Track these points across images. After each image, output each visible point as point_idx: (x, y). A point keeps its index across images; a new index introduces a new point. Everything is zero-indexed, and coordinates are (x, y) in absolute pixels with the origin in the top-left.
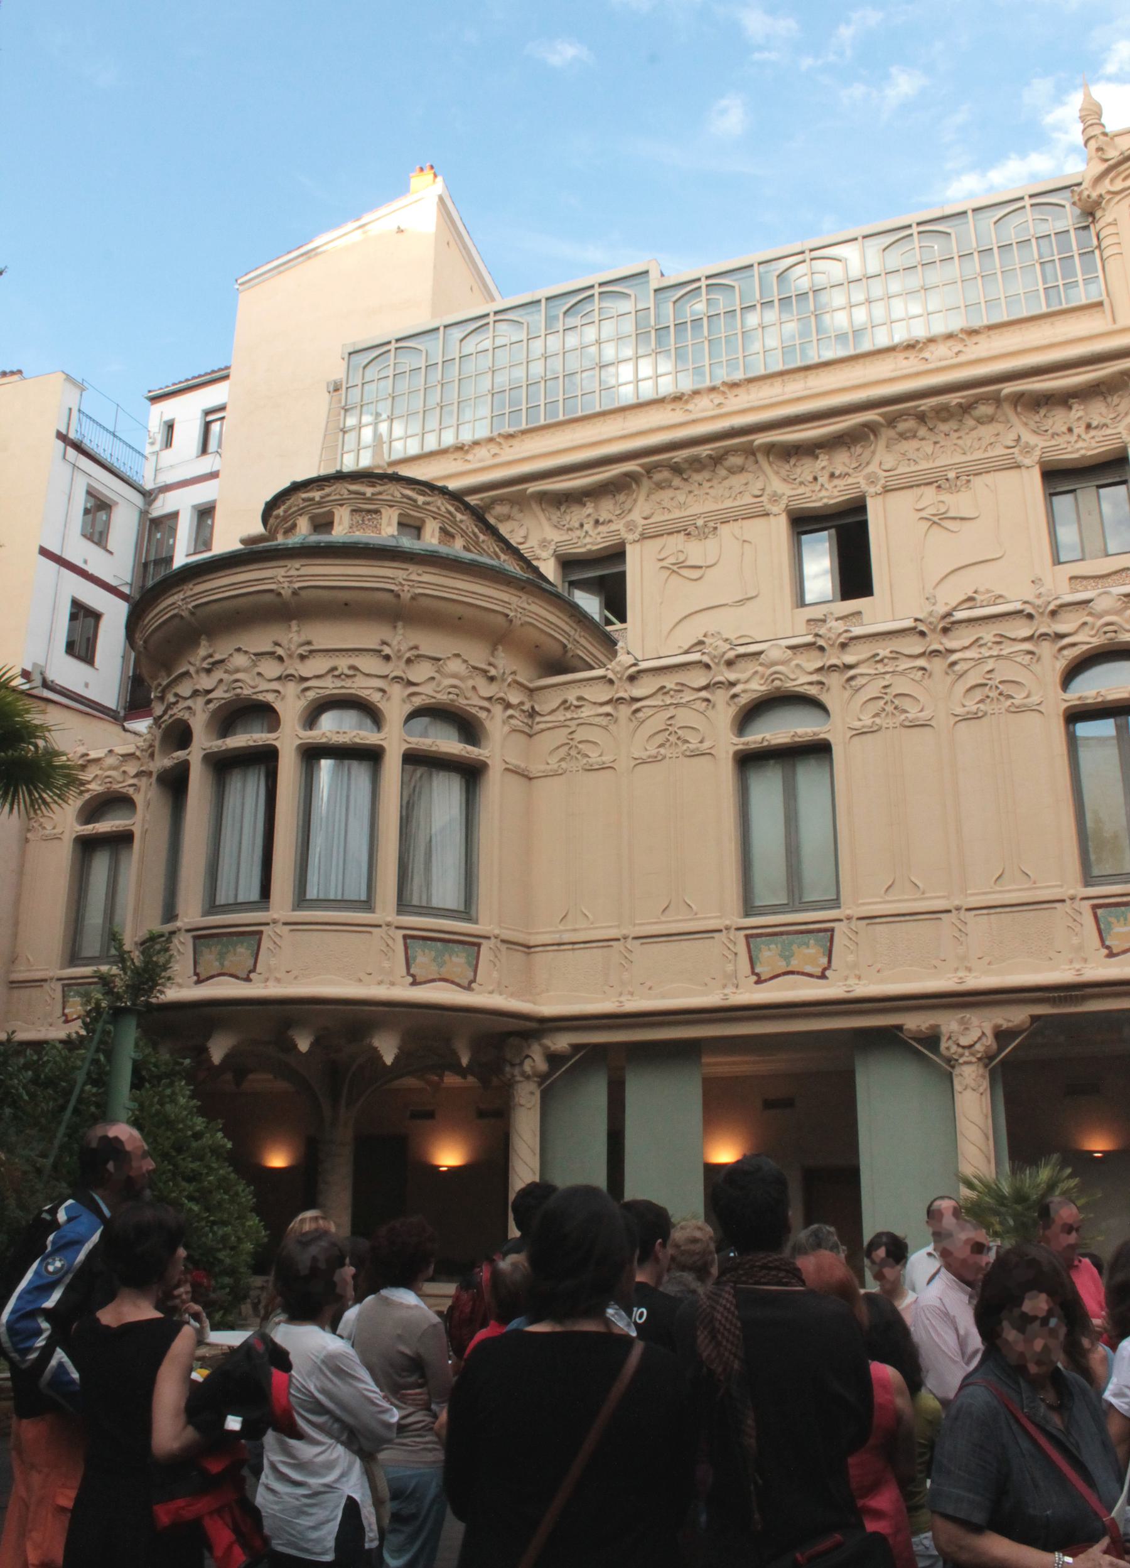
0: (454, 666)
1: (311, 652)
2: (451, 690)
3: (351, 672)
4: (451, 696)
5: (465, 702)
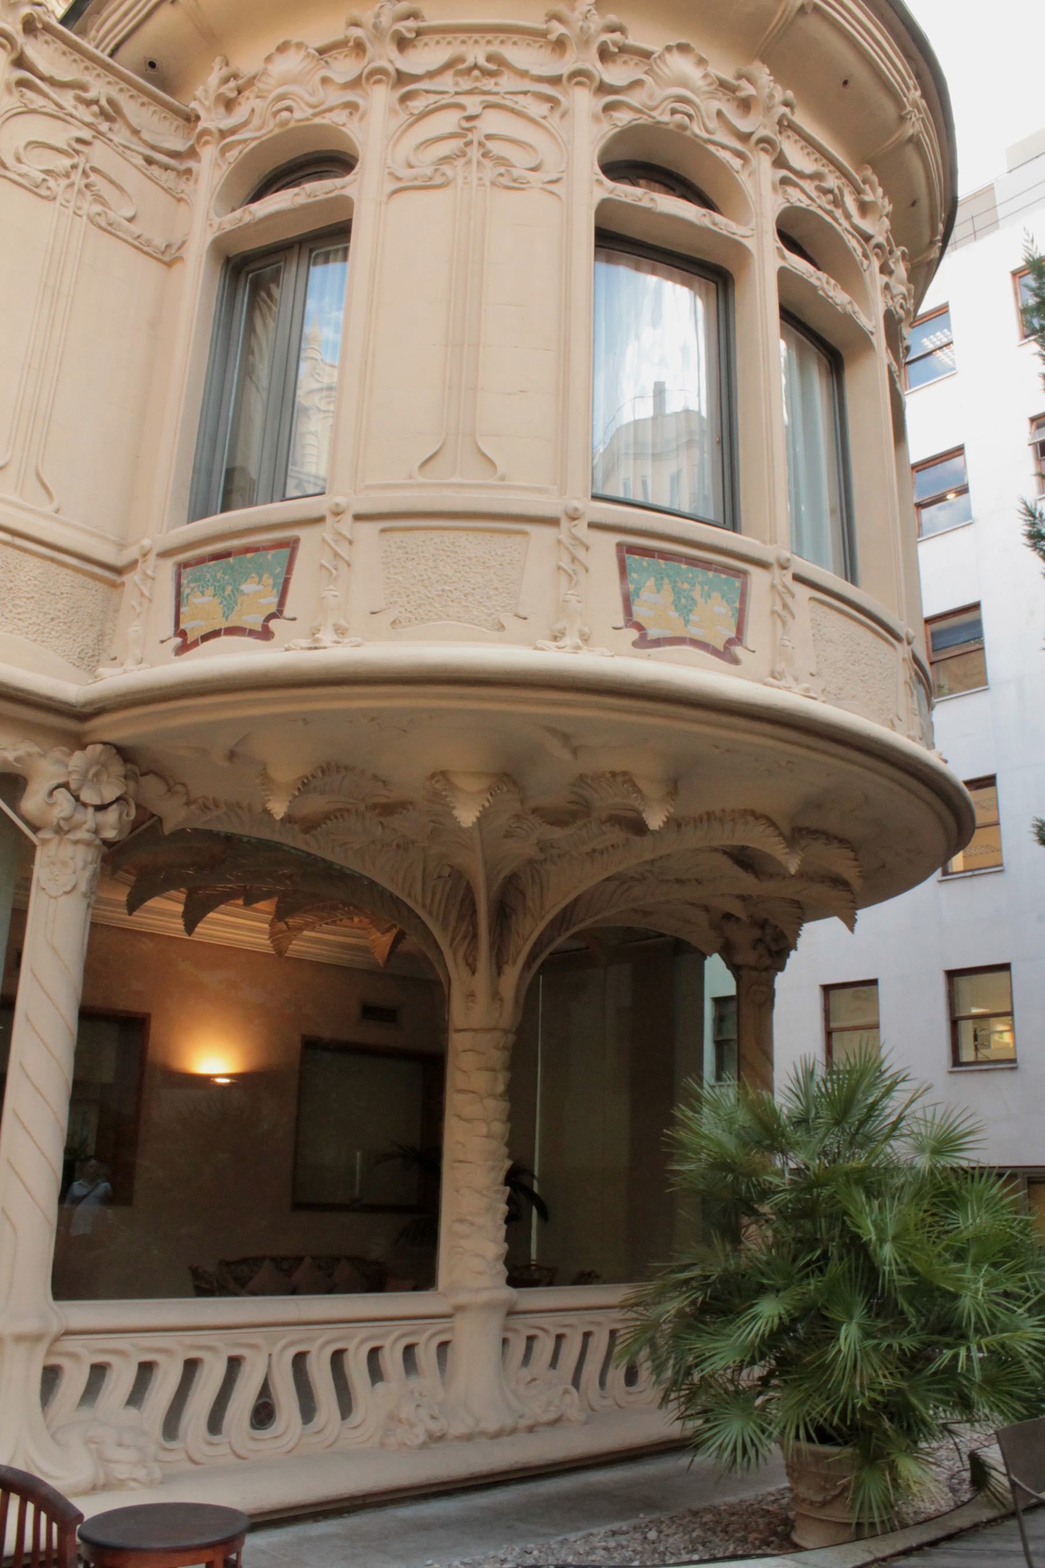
0: (681, 65)
1: (419, 33)
2: (678, 106)
3: (492, 67)
4: (678, 117)
5: (704, 135)
